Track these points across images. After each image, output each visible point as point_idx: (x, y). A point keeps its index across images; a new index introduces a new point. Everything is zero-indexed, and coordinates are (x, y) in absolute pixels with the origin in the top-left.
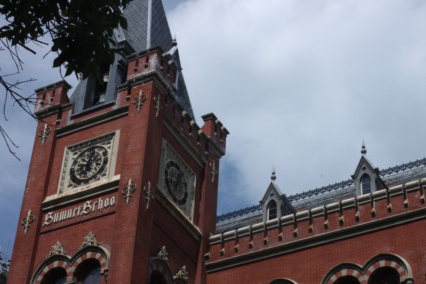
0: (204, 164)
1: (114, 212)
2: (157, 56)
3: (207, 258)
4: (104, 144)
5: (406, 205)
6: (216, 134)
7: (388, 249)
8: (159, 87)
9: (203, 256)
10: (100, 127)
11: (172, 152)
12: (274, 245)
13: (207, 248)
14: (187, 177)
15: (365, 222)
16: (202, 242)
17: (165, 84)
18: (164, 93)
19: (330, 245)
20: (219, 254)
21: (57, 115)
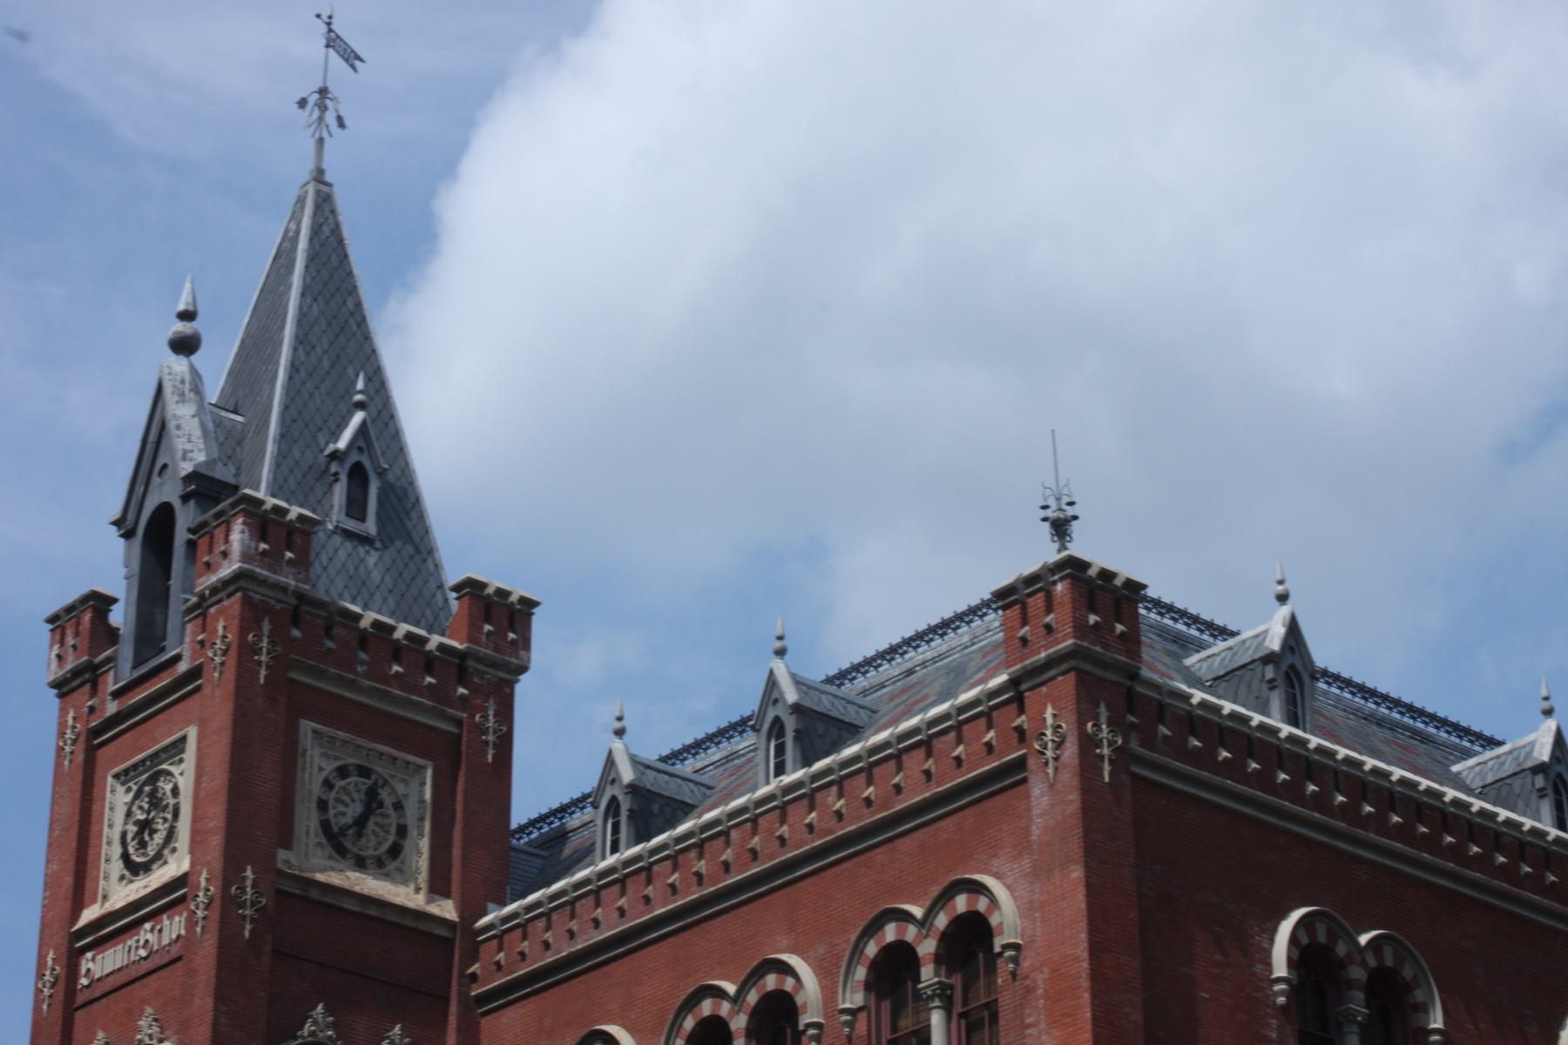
0: (459, 722)
1: (179, 959)
2: (244, 523)
3: (474, 977)
4: (172, 764)
5: (810, 827)
6: (487, 627)
7: (784, 941)
8: (264, 598)
9: (462, 974)
10: (163, 716)
11: (338, 744)
12: (588, 940)
13: (473, 955)
14: (404, 781)
15: (740, 875)
16: (458, 939)
17: (282, 584)
18: (285, 606)
19: (686, 935)
20: (494, 968)
21: (88, 687)
